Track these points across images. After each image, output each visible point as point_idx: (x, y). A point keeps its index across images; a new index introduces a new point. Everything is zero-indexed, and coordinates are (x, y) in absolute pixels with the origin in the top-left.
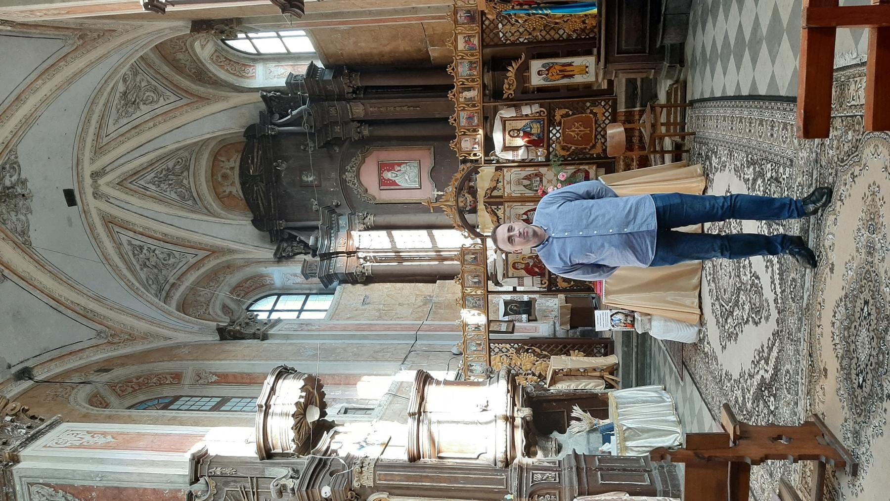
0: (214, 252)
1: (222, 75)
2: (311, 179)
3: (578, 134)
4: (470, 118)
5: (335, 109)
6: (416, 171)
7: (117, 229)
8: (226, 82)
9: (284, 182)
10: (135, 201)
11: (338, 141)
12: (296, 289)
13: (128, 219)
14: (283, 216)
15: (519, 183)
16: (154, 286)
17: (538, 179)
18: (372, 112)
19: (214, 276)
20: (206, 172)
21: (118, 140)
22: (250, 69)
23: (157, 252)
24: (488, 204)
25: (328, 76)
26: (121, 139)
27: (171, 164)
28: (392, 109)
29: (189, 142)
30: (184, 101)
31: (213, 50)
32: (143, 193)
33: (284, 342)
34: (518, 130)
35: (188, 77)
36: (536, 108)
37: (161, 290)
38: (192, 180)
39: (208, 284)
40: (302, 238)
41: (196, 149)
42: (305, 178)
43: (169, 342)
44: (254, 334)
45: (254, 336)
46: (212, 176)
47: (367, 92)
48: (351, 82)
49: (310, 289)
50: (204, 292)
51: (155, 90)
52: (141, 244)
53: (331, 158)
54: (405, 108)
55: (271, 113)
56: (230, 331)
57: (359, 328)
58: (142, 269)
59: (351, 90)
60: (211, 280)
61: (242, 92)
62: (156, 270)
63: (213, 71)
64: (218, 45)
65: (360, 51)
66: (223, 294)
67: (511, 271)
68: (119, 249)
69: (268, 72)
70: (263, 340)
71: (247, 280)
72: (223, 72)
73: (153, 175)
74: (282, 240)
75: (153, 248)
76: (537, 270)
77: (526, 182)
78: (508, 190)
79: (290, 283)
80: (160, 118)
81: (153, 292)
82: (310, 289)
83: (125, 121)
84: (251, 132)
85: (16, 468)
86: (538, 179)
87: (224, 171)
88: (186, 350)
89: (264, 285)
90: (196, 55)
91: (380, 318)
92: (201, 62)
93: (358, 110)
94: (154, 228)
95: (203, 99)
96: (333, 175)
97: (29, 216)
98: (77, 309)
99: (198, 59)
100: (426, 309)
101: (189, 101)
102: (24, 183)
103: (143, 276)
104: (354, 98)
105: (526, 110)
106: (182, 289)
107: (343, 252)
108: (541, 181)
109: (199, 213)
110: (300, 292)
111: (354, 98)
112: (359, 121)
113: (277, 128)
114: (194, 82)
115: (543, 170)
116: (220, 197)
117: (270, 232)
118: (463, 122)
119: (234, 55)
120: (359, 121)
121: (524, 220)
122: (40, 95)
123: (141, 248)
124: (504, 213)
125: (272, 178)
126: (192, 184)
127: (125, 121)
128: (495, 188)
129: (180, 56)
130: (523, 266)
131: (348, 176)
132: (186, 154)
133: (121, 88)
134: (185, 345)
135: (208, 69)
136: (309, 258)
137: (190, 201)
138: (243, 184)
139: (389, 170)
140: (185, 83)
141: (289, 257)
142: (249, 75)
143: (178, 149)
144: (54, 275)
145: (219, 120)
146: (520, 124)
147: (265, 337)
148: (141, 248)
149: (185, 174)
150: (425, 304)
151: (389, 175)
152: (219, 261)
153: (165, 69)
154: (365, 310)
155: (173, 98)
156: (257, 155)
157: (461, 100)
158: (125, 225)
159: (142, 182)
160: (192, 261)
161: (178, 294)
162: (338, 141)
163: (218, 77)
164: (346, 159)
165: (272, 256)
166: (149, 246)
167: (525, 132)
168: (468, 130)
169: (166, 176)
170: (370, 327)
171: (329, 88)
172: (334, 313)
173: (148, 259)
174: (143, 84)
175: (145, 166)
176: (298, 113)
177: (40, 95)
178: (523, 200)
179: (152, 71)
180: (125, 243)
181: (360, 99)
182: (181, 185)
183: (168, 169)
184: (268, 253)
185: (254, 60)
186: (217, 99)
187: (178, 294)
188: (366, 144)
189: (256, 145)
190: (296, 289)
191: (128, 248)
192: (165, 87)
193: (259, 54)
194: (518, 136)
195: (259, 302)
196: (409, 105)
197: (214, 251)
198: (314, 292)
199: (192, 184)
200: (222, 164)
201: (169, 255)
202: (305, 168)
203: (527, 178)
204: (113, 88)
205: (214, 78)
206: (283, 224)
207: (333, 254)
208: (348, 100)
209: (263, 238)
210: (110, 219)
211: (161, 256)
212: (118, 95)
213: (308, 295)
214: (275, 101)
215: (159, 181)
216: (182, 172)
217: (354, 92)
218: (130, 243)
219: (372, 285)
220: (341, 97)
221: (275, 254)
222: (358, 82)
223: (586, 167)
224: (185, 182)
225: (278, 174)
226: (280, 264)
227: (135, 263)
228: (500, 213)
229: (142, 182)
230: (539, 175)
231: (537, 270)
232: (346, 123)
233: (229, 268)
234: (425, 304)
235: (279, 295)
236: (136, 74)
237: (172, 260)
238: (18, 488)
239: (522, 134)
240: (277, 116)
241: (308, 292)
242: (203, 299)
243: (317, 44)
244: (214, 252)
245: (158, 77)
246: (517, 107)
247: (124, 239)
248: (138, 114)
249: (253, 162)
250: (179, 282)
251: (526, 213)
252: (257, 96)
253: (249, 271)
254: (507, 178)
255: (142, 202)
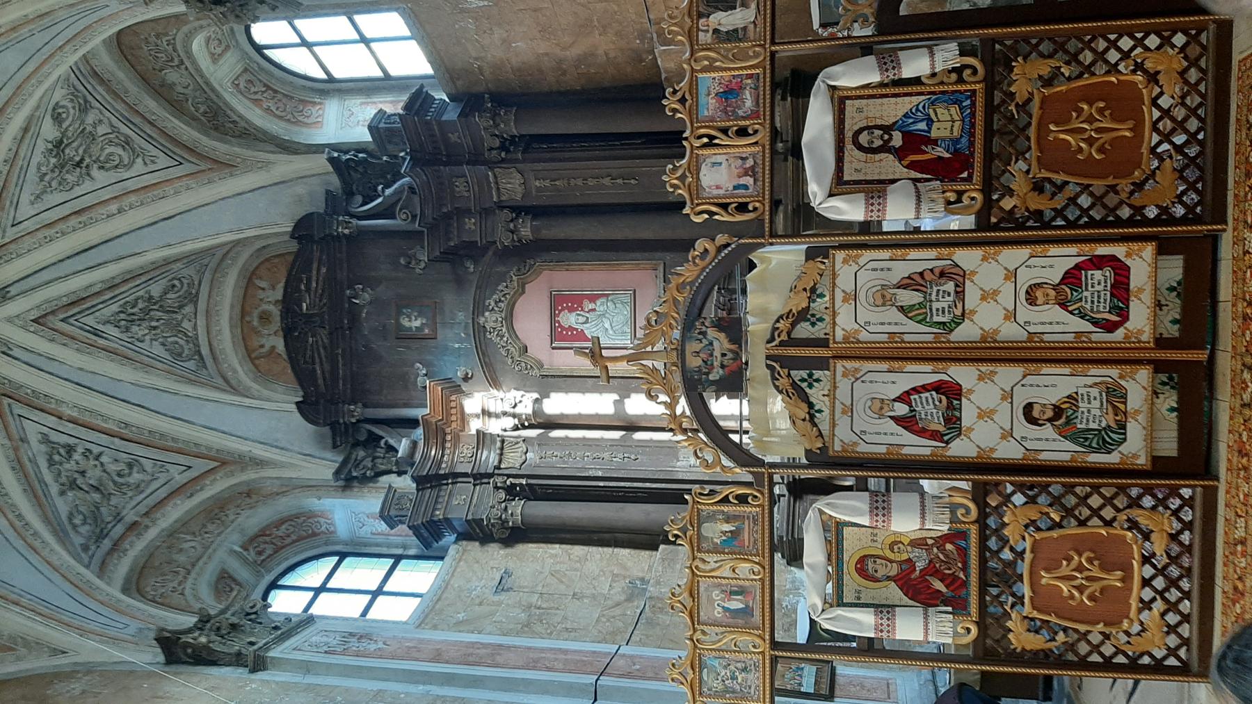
0: (224, 463)
1: (256, 117)
2: (417, 323)
3: (1091, 142)
4: (729, 93)
5: (465, 182)
6: (627, 311)
7: (19, 409)
8: (265, 133)
9: (367, 326)
10: (70, 357)
11: (472, 251)
12: (377, 545)
13: (49, 391)
14: (359, 395)
15: (884, 298)
16: (84, 529)
17: (950, 286)
18: (539, 189)
19: (216, 511)
20: (232, 306)
21: (40, 235)
22: (314, 110)
23: (104, 459)
24: (779, 363)
25: (452, 114)
26: (47, 232)
27: (156, 290)
28: (580, 182)
29: (189, 247)
30: (187, 168)
31: (239, 68)
32: (92, 341)
33: (298, 678)
34: (887, 129)
35: (192, 120)
36: (947, 55)
37: (101, 536)
38: (201, 322)
39: (204, 526)
40: (392, 442)
41: (210, 261)
42: (405, 322)
43: (61, 661)
44: (239, 654)
45: (237, 660)
46: (243, 317)
47: (531, 143)
48: (496, 125)
49: (405, 547)
50: (190, 544)
51: (127, 143)
52: (72, 441)
53: (460, 282)
54: (607, 181)
55: (349, 194)
56: (187, 645)
57: (469, 656)
58: (62, 493)
59: (497, 143)
60: (212, 520)
61: (296, 152)
62: (96, 496)
63: (240, 109)
64: (250, 58)
65: (515, 61)
66: (225, 550)
67: (852, 581)
68: (16, 449)
69: (347, 113)
70: (254, 670)
71: (282, 521)
72: (258, 111)
73: (115, 308)
74: (356, 444)
75: (96, 450)
76: (939, 585)
77: (909, 297)
78: (845, 322)
79: (365, 532)
80: (133, 198)
81: (78, 540)
82: (405, 547)
83: (59, 197)
84: (304, 229)
86: (950, 286)
87: (265, 307)
88: (76, 687)
89: (314, 534)
90: (198, 70)
91: (526, 628)
92: (213, 90)
93: (512, 184)
94: (104, 411)
95: (225, 166)
96: (461, 316)
99: (208, 83)
100: (632, 610)
101: (194, 168)
103: (63, 506)
104: (503, 161)
105: (915, 65)
106: (152, 533)
107: (465, 475)
108: (960, 294)
109: (203, 385)
110: (384, 551)
111: (503, 161)
112: (513, 209)
113: (354, 221)
114: (208, 135)
115: (967, 258)
116: (252, 356)
117: (334, 426)
118: (709, 105)
119: (283, 82)
120: (513, 209)
121: (898, 420)
123: (70, 449)
124: (832, 395)
125: (344, 320)
126: (201, 331)
127: (59, 197)
128: (803, 315)
129: (172, 76)
130: (894, 570)
131: (490, 319)
132: (191, 271)
133: (49, 131)
134: (89, 669)
135: (226, 103)
136: (405, 483)
137: (194, 362)
138: (287, 332)
139: (571, 310)
140: (188, 133)
141: (365, 480)
142: (309, 121)
143: (167, 262)
145: (251, 206)
146: (893, 109)
147: (258, 664)
148: (70, 449)
149: (188, 309)
150: (629, 599)
151: (570, 319)
152: (233, 481)
153: (150, 105)
154: (500, 603)
155: (163, 161)
156: (318, 274)
157: (706, 38)
158: (41, 403)
159: (90, 320)
160: (180, 478)
161: (137, 548)
162: (472, 251)
163: (247, 122)
164: (486, 285)
165: (330, 476)
166: (89, 446)
167: (907, 135)
168: (725, 131)
169: (146, 311)
170: (492, 656)
171: (453, 138)
172: (433, 609)
173: (83, 473)
174: (101, 130)
175: (96, 289)
176: (395, 192)
178: (896, 354)
179: (120, 106)
180: (33, 439)
181: (517, 161)
182: (177, 329)
183: (151, 297)
184: (324, 467)
185: (324, 93)
186: (252, 166)
187: (137, 548)
188: (526, 255)
189: (317, 254)
190: (377, 545)
191: (37, 448)
192: (149, 139)
193: (331, 79)
194: (885, 148)
195: (300, 570)
196: (615, 172)
197: (224, 461)
198: (412, 552)
199: (201, 331)
200: (261, 294)
201: (130, 466)
202: (405, 303)
203: (908, 283)
204: (26, 130)
205: (243, 124)
206: (358, 411)
207: (446, 476)
208: (491, 164)
209: (320, 440)
210: (8, 391)
211: (113, 468)
212: (41, 146)
213: (398, 559)
214: (355, 170)
215: (128, 319)
216: (181, 307)
217: (503, 147)
218: (45, 440)
219: (521, 548)
220: (476, 158)
221: (337, 473)
222: (511, 128)
223: (1119, 250)
224: (186, 325)
225: (354, 313)
226: (348, 493)
227: (48, 477)
228: (817, 394)
229: (90, 320)
230: (957, 276)
231: (939, 585)
232: (485, 213)
233: (249, 495)
234: (629, 599)
235: (343, 556)
236: (84, 108)
237: (136, 477)
239: (897, 140)
240: (359, 199)
241: (399, 551)
242: (182, 558)
243: (434, 56)
244: (224, 463)
245: (137, 120)
246: (888, 60)
247: (32, 431)
248: (88, 186)
249: (308, 289)
250: (146, 521)
251: (904, 398)
252: (320, 163)
253: (285, 505)
254: (845, 280)
255: (85, 358)
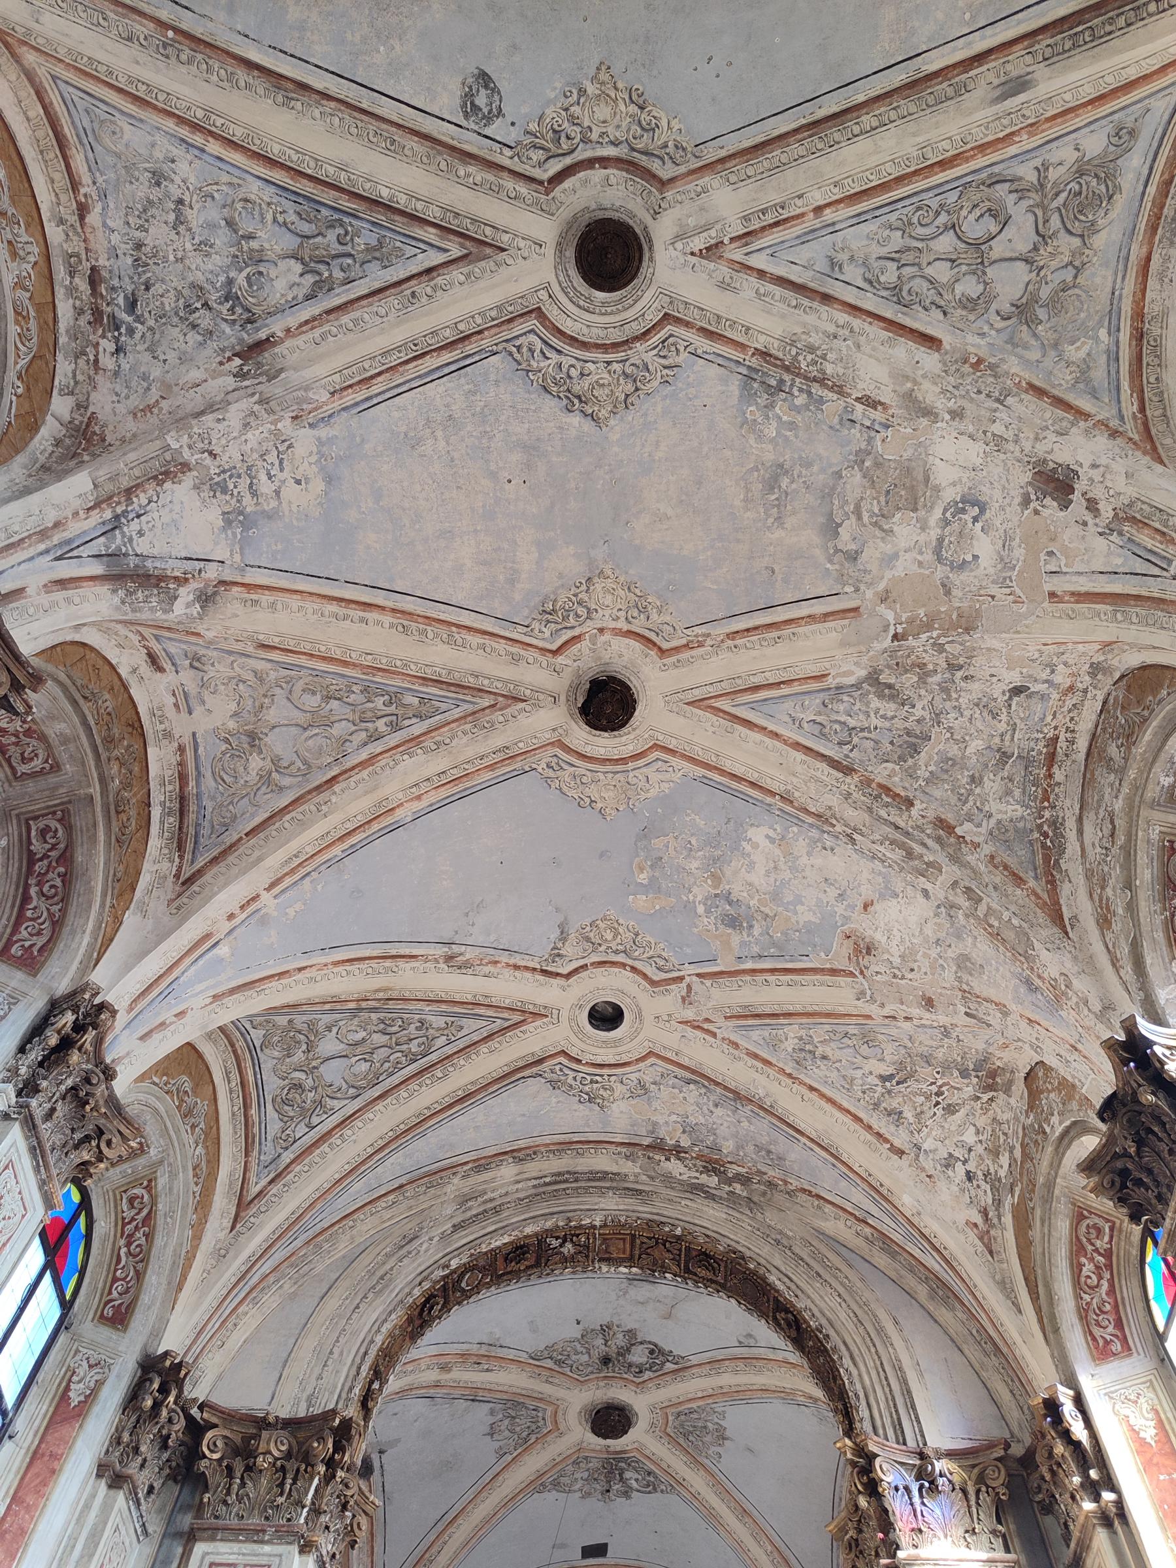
85: (295, 1549)
97: (579, 1494)
98: (434, 1550)
102: (626, 1494)
122: (749, 1542)
144: (487, 1520)
177: (749, 1542)
238: (267, 1548)
